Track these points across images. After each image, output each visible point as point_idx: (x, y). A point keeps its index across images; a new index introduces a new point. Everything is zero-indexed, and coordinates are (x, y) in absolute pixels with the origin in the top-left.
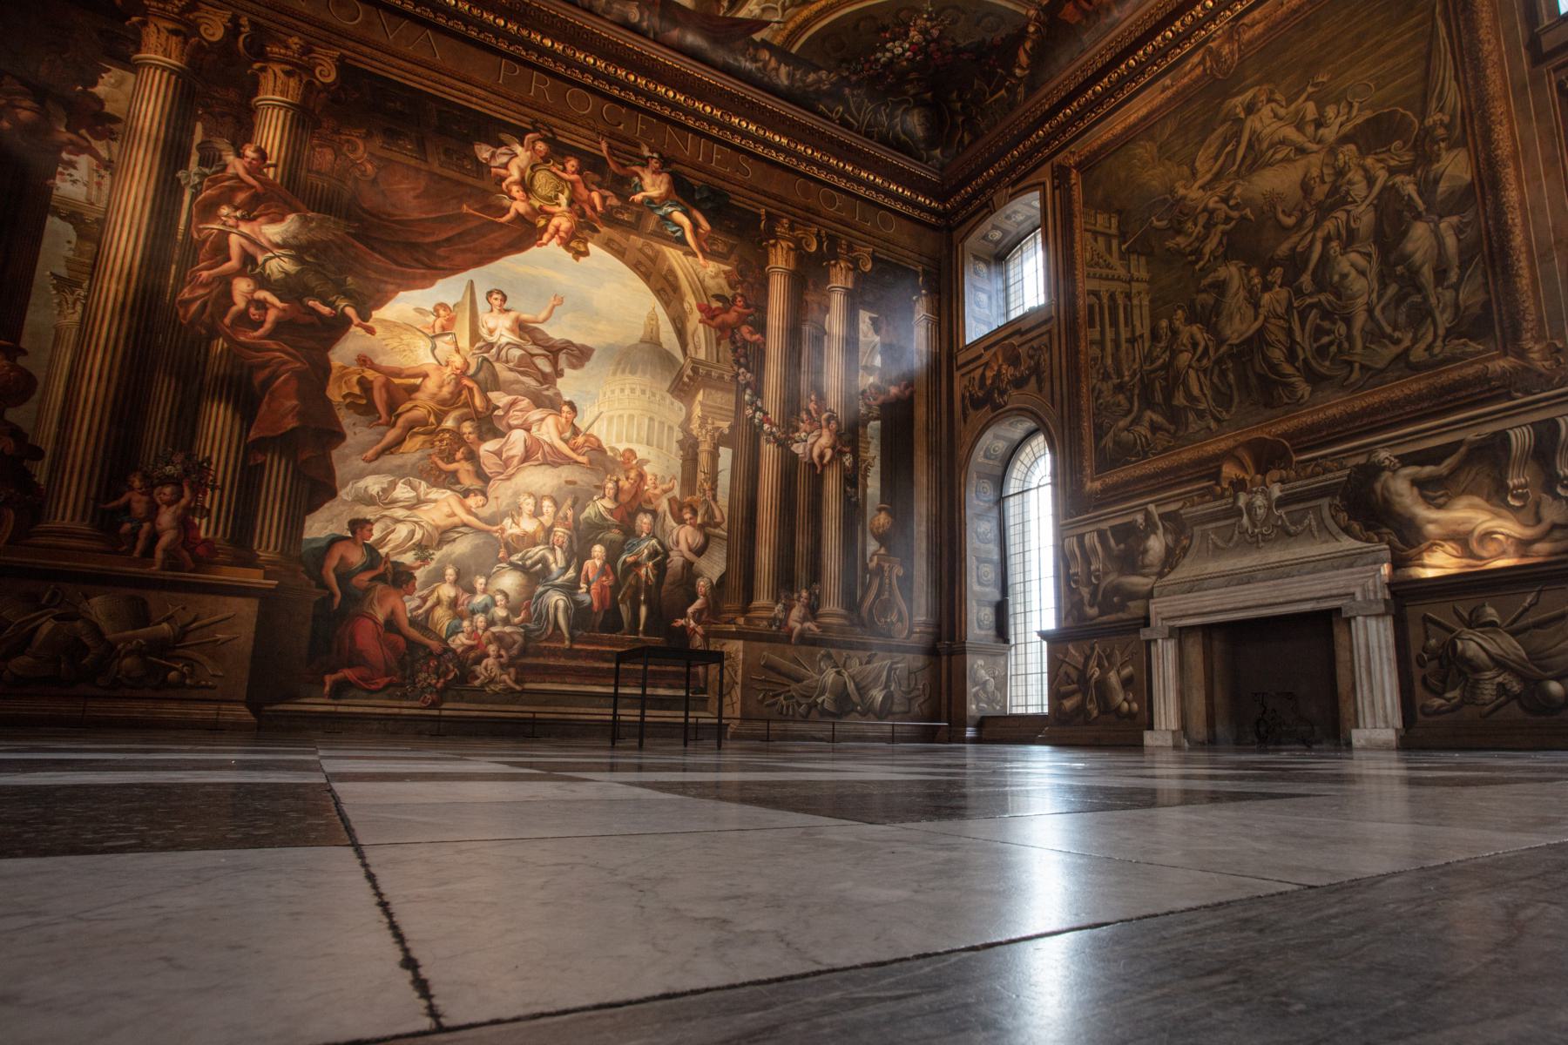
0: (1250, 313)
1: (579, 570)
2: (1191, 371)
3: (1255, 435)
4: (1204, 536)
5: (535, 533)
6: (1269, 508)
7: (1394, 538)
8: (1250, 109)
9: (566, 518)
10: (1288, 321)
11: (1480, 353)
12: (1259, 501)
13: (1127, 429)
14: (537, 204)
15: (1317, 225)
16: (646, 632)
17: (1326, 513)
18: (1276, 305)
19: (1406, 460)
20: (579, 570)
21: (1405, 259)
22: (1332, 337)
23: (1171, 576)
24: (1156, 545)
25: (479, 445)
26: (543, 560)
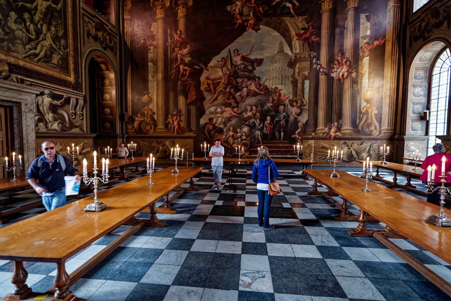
1: (264, 124)
5: (251, 115)
9: (259, 110)
14: (244, 19)
16: (283, 139)
20: (264, 124)
25: (235, 94)
26: (254, 123)
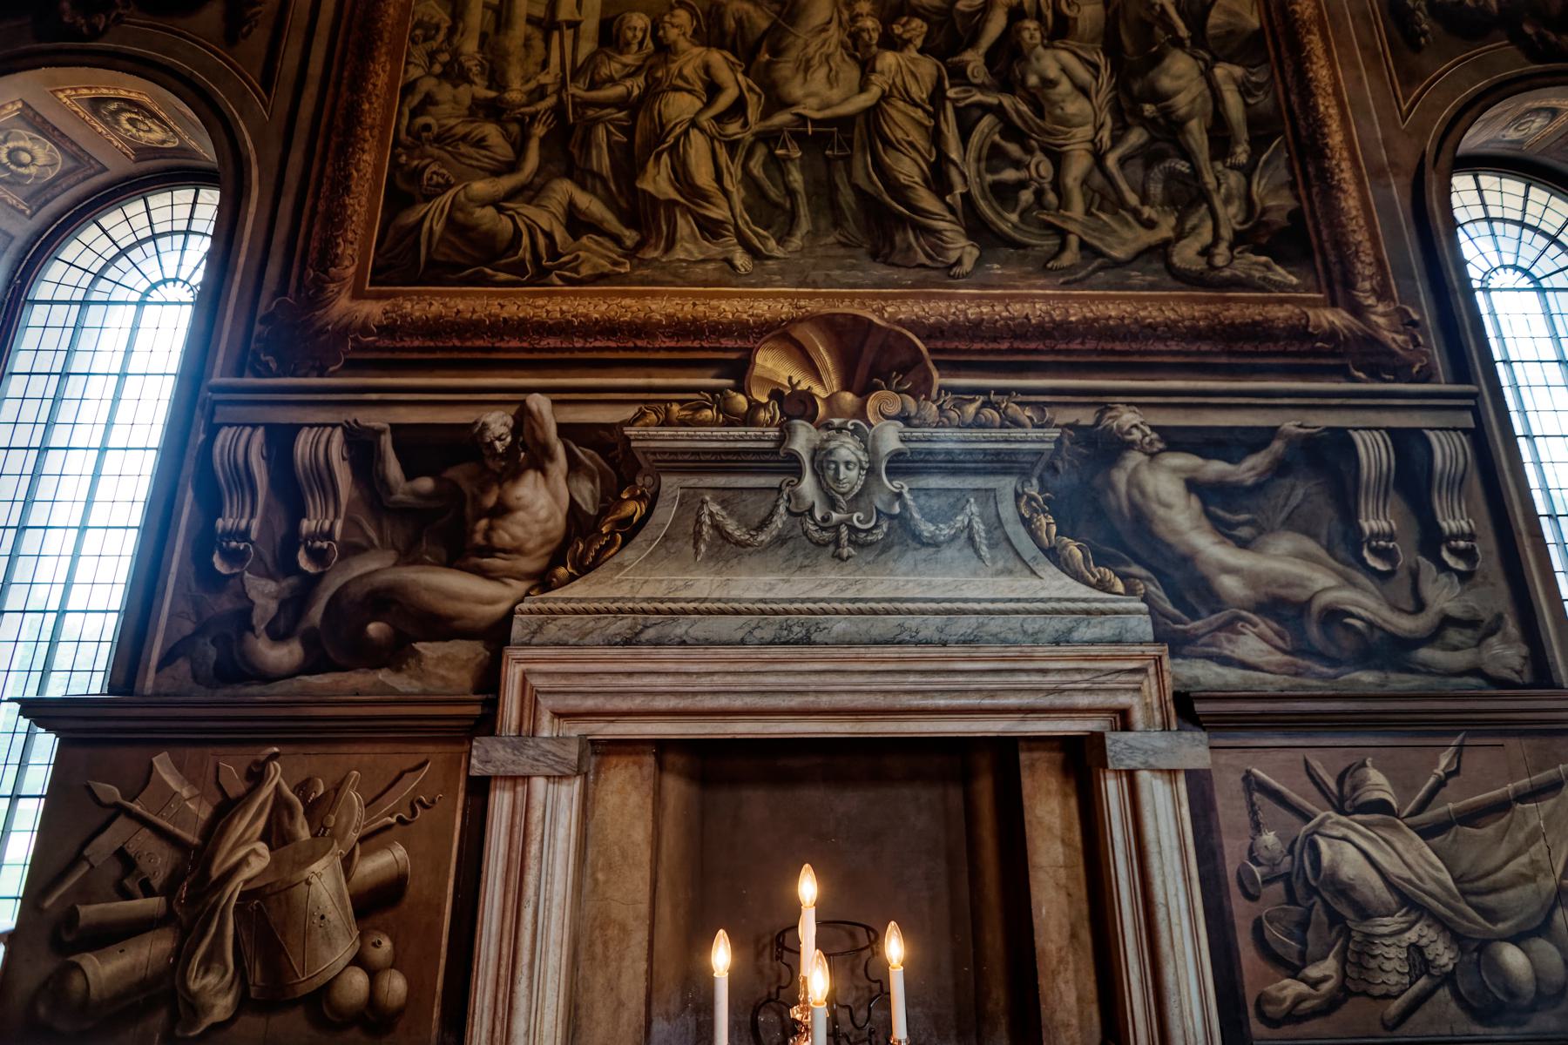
0: (851, 73)
3: (844, 308)
4: (690, 502)
6: (872, 471)
7: (1156, 590)
10: (934, 116)
11: (1295, 288)
12: (847, 449)
13: (497, 203)
17: (1008, 510)
18: (909, 79)
19: (1174, 440)
21: (1158, 97)
22: (1023, 174)
23: (578, 590)
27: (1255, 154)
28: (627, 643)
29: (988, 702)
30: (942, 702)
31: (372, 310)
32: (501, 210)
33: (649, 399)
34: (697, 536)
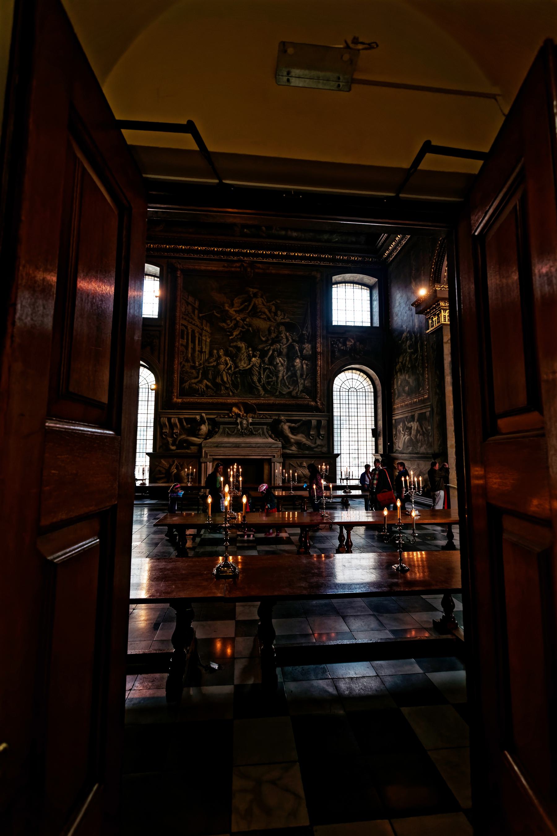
2: (224, 372)
4: (224, 429)
6: (248, 425)
8: (255, 295)
12: (245, 422)
13: (195, 383)
15: (272, 345)
17: (265, 430)
19: (288, 421)
23: (210, 440)
24: (204, 428)
27: (306, 377)
28: (216, 447)
29: (259, 455)
30: (253, 454)
31: (180, 400)
32: (196, 385)
33: (218, 414)
34: (225, 433)
